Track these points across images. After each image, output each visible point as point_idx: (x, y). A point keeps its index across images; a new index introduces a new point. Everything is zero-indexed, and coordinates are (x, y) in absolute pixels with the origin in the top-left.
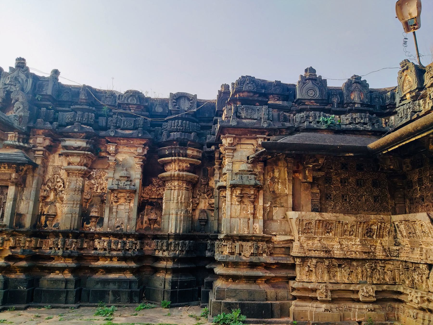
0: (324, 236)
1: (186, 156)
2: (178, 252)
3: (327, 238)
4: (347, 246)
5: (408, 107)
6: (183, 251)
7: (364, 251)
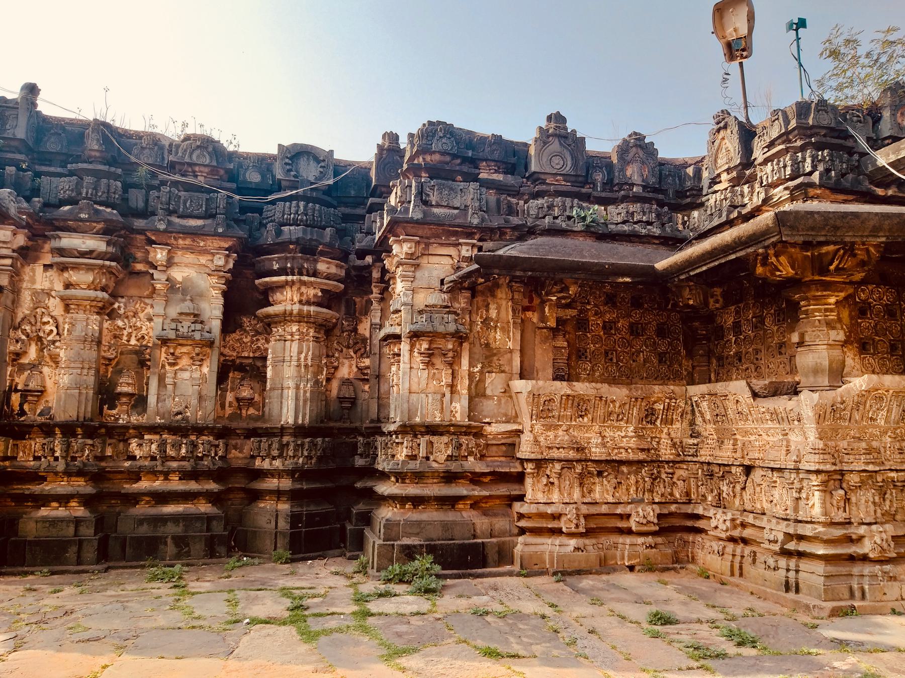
0: (574, 423)
1: (315, 274)
2: (301, 460)
3: (581, 426)
4: (613, 439)
5: (723, 197)
6: (311, 458)
7: (641, 447)
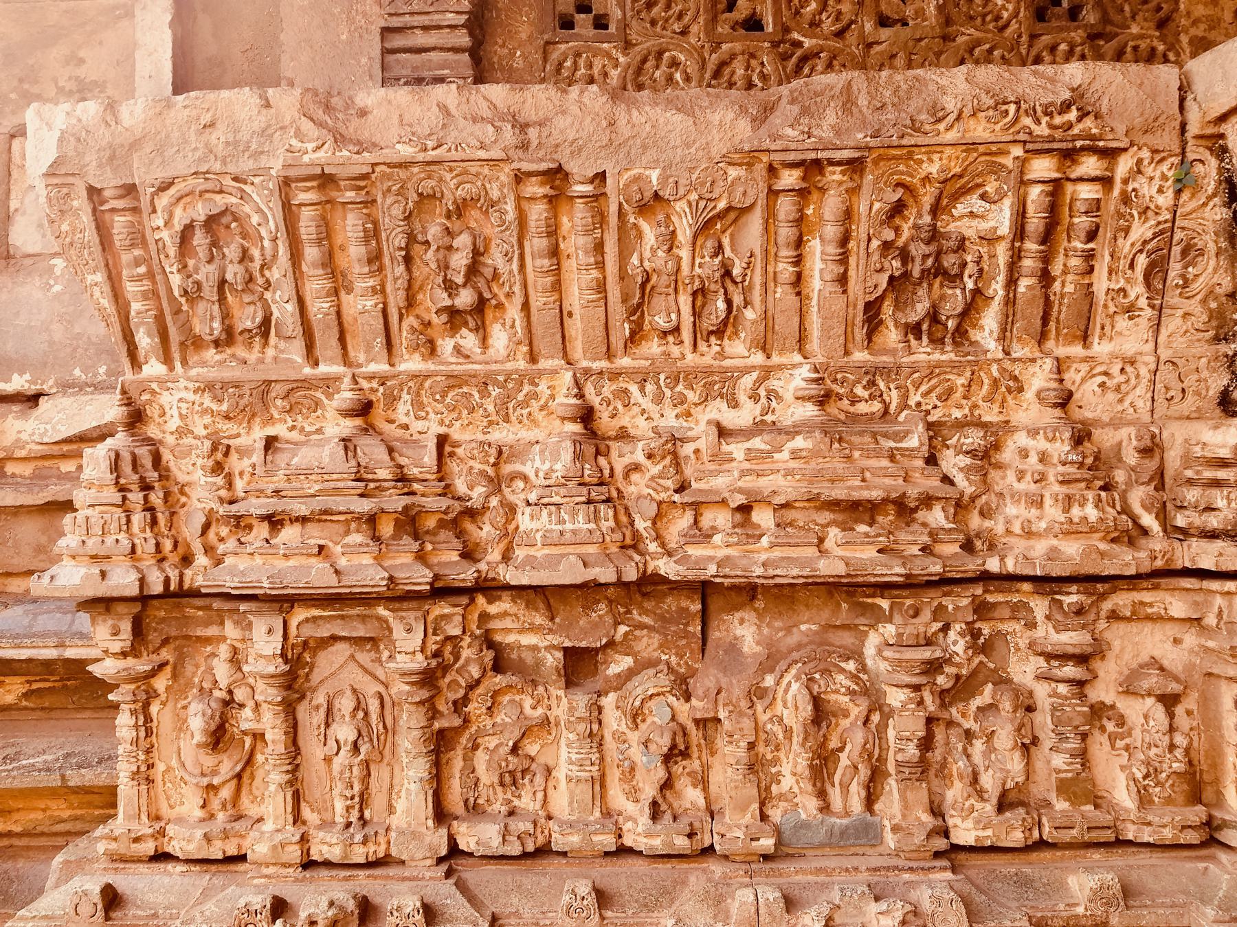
3: (455, 380)
4: (670, 448)
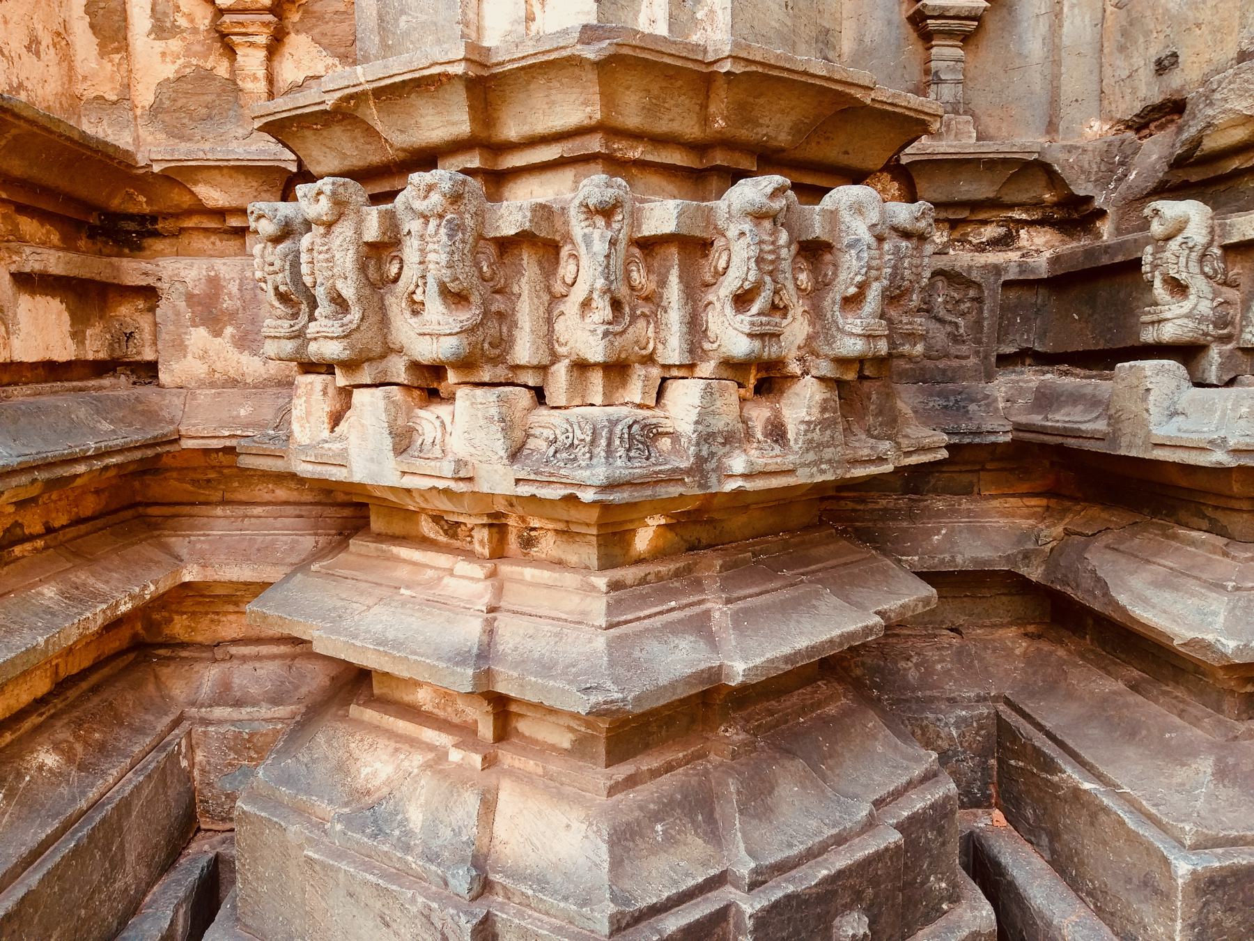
2: (684, 405)
6: (767, 378)
